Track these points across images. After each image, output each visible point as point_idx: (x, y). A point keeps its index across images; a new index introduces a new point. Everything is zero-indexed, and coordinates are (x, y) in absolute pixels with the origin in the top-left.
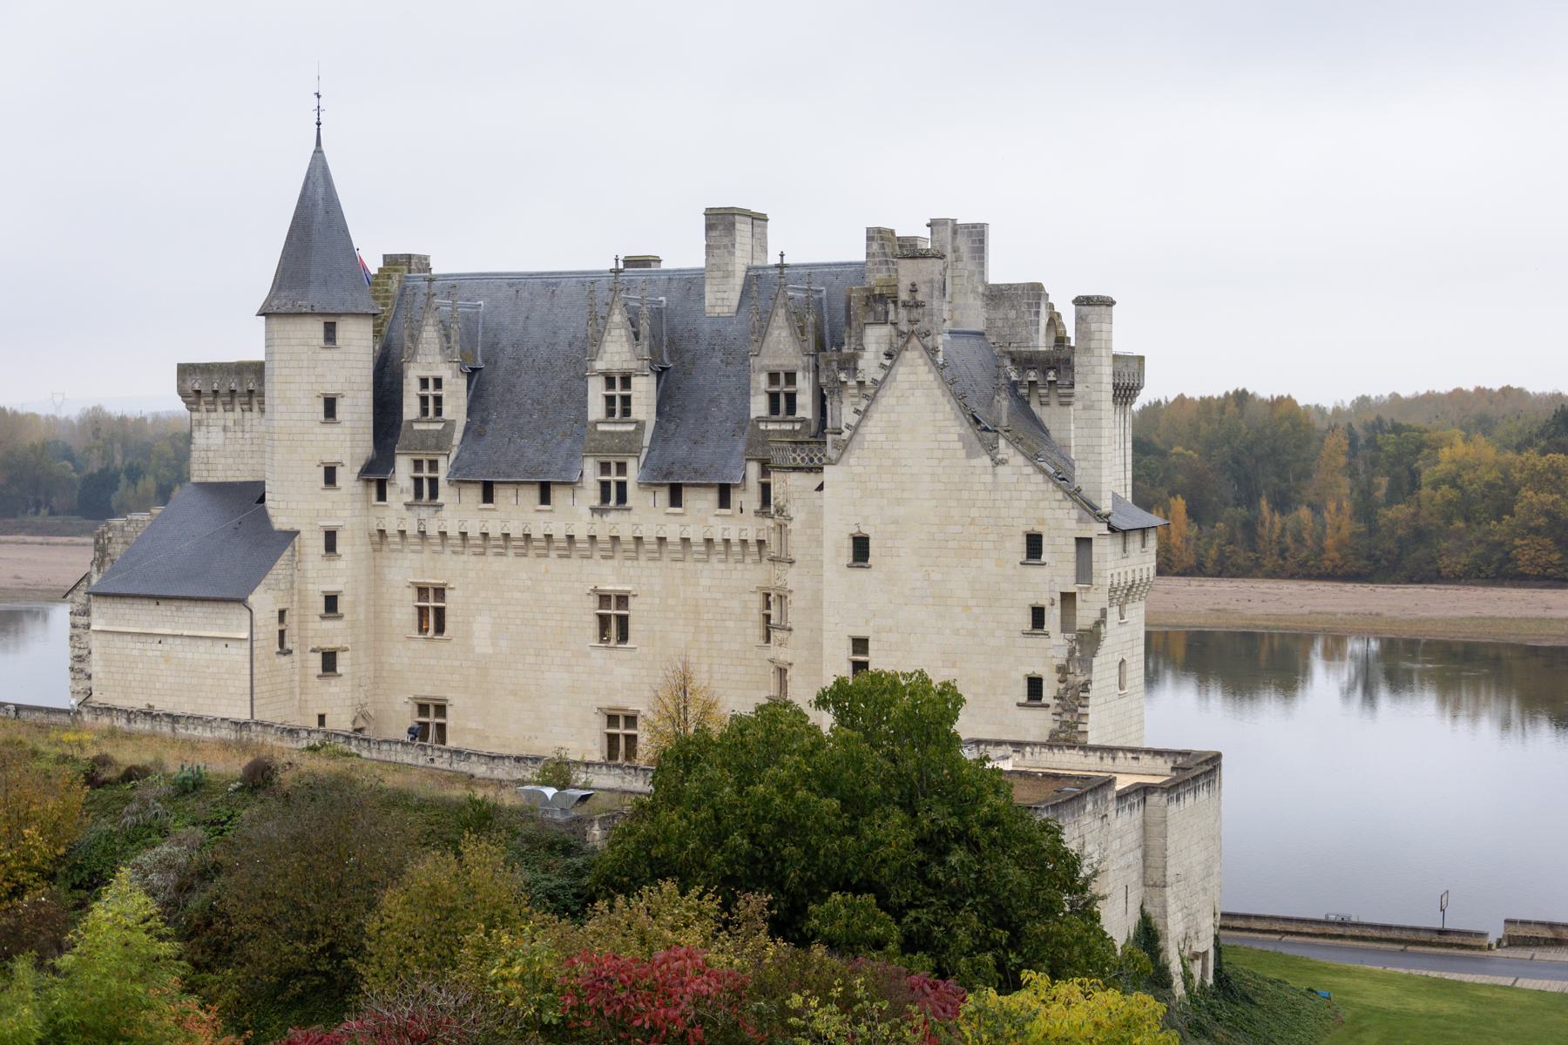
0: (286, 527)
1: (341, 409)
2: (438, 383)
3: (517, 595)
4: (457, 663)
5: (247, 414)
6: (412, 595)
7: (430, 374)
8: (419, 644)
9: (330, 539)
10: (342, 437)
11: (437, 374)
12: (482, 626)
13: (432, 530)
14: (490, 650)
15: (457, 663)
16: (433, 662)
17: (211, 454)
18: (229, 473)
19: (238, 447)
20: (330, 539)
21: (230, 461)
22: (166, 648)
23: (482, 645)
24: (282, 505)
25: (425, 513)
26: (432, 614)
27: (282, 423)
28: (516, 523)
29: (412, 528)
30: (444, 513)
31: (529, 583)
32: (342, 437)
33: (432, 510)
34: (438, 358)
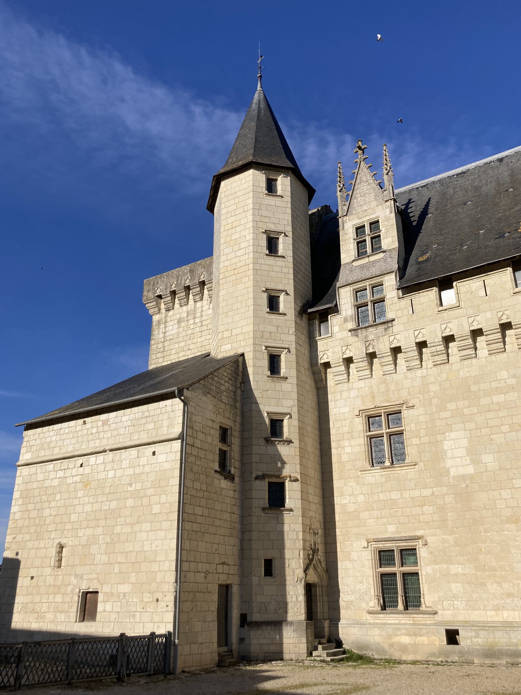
0: (231, 353)
1: (285, 246)
2: (375, 224)
3: (501, 398)
4: (427, 492)
5: (199, 304)
6: (360, 424)
7: (365, 220)
8: (376, 475)
9: (274, 364)
10: (285, 270)
11: (372, 217)
12: (455, 447)
13: (383, 347)
14: (470, 470)
15: (427, 492)
16: (395, 495)
17: (167, 344)
18: (180, 355)
19: (189, 332)
20: (274, 364)
21: (183, 344)
22: (87, 470)
23: (457, 461)
24: (226, 334)
25: (372, 333)
26: (386, 436)
27: (227, 263)
28: (489, 315)
29: (357, 350)
30: (397, 327)
31: (513, 381)
32: (285, 270)
33: (381, 328)
34: (374, 203)
